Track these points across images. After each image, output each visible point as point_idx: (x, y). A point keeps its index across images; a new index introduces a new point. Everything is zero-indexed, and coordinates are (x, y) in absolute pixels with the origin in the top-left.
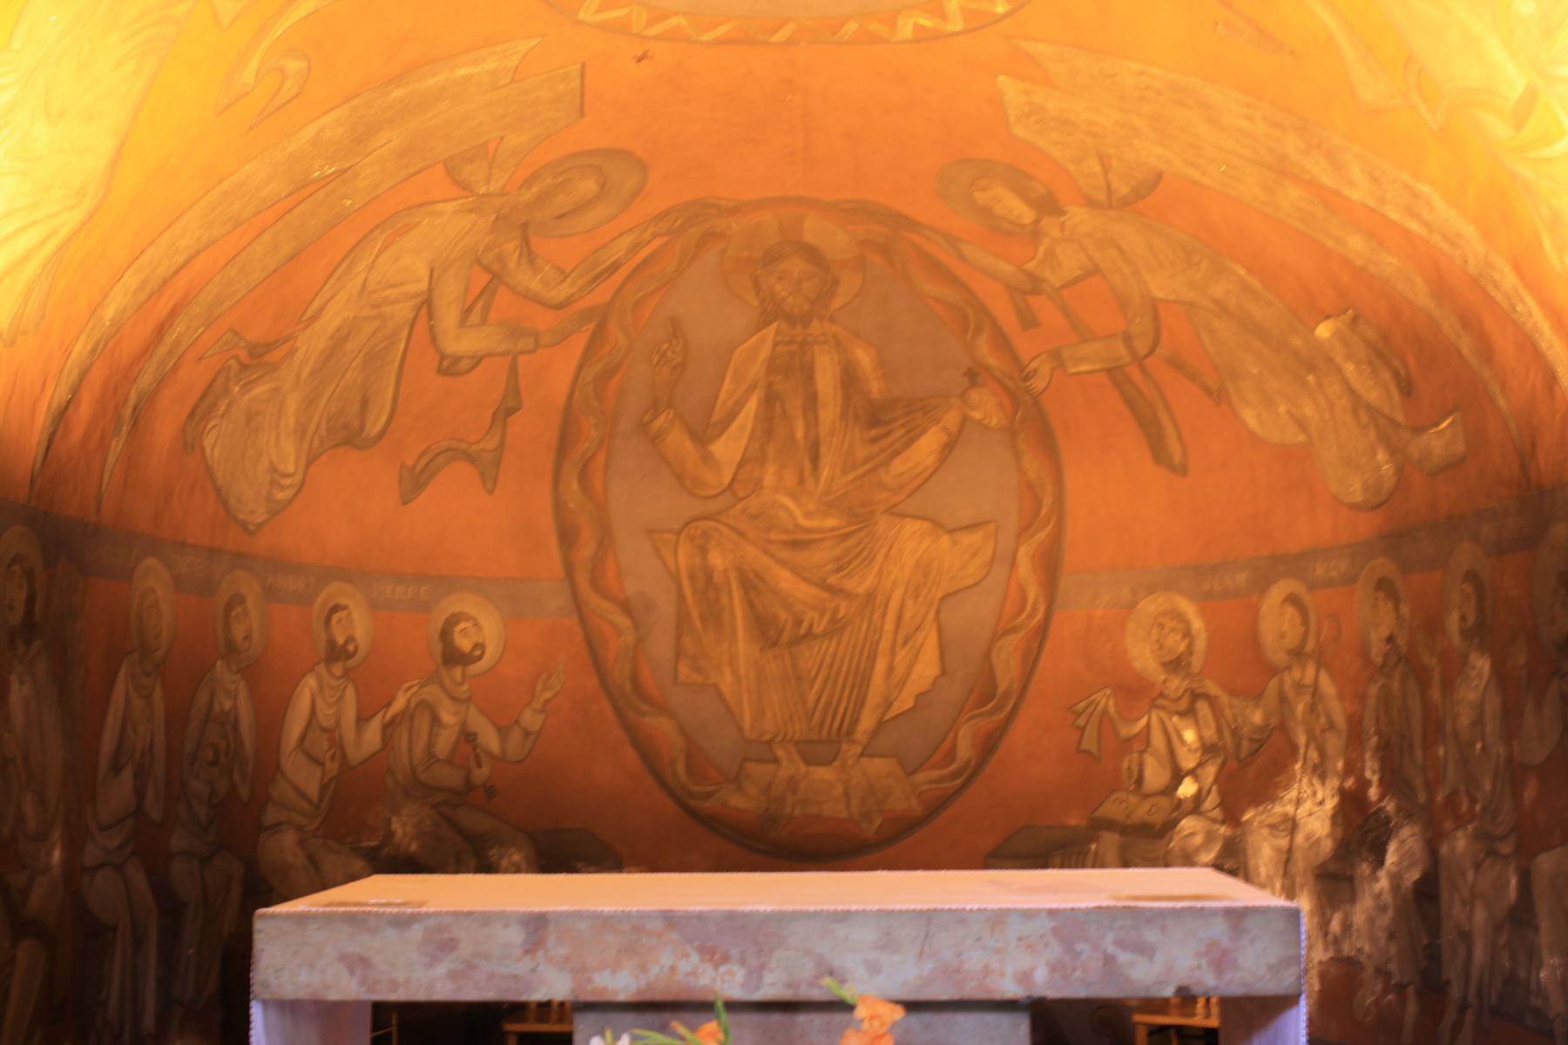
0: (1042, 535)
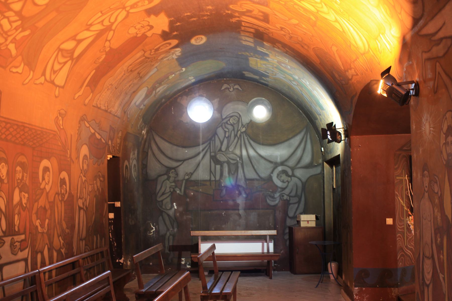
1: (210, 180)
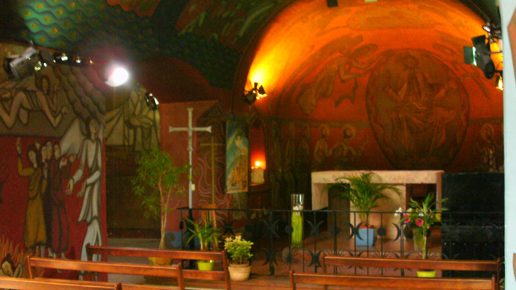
1: (124, 145)
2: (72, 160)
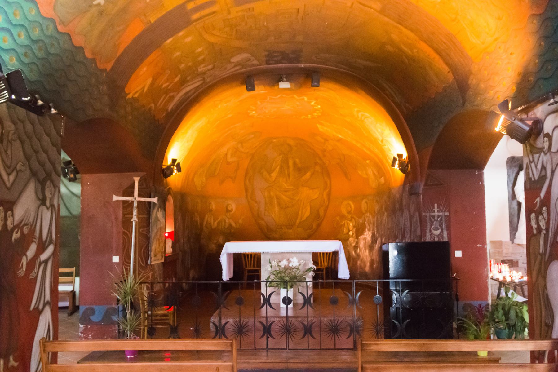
0: (327, 190)
2: (26, 231)
